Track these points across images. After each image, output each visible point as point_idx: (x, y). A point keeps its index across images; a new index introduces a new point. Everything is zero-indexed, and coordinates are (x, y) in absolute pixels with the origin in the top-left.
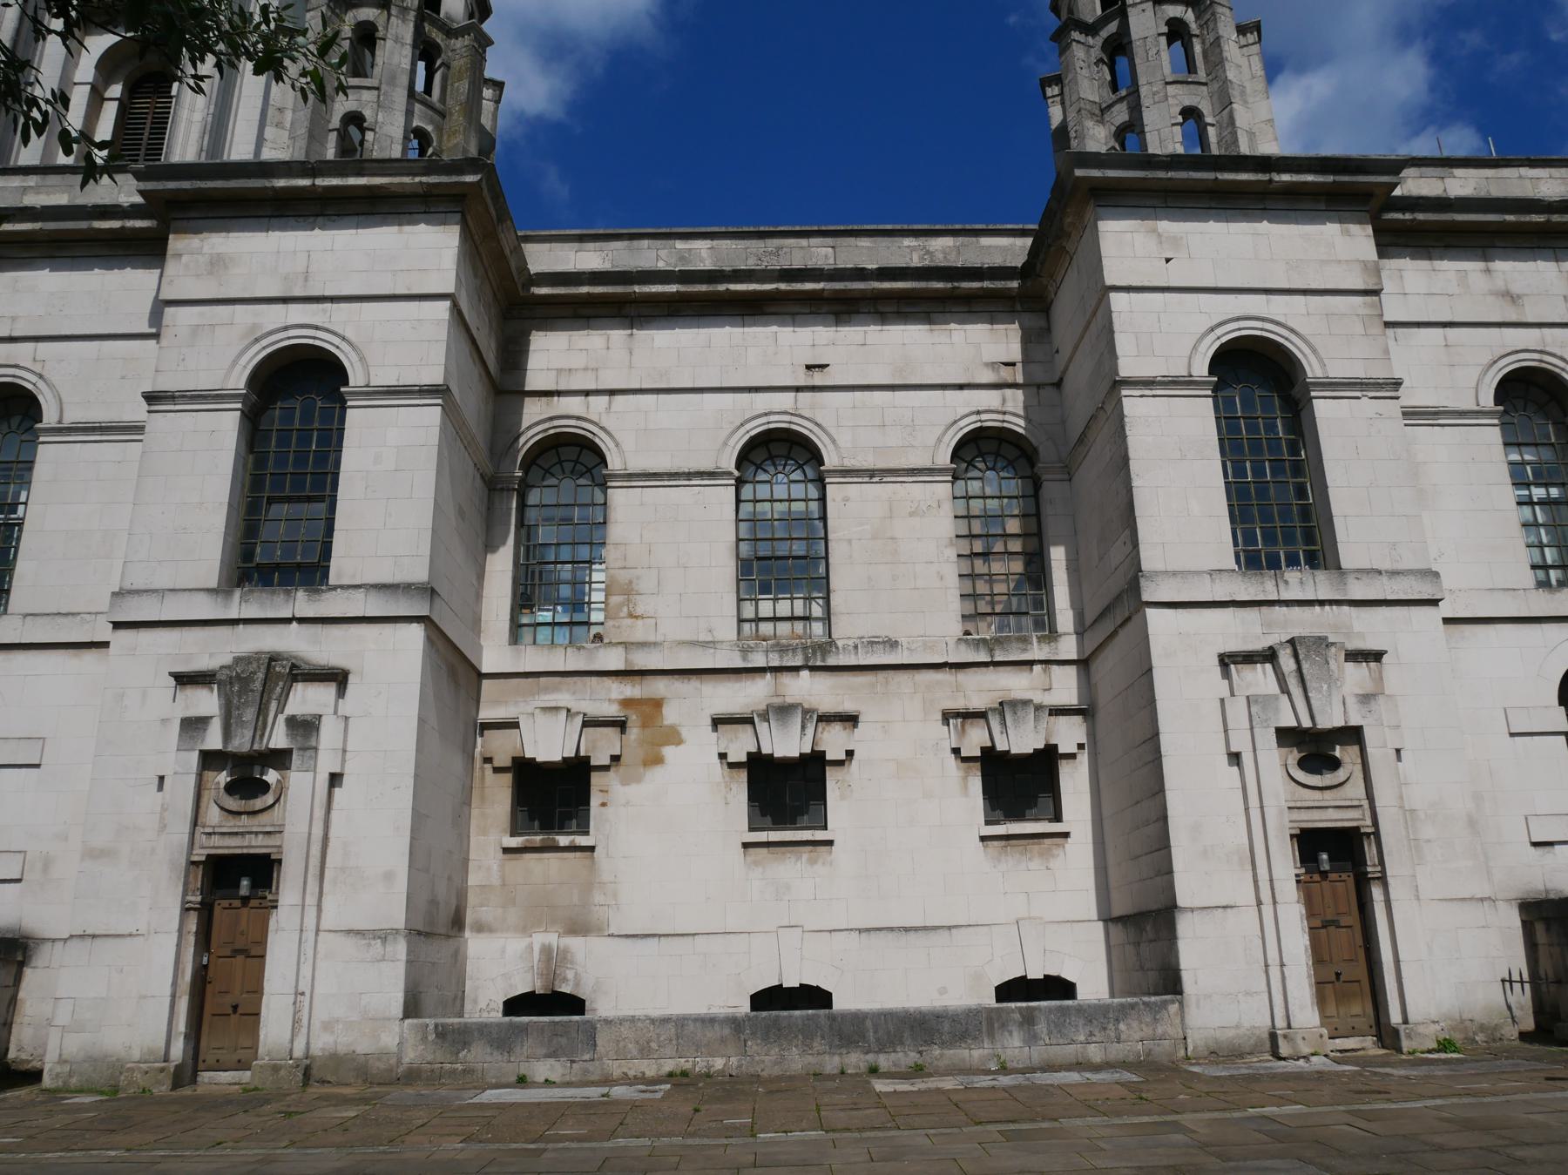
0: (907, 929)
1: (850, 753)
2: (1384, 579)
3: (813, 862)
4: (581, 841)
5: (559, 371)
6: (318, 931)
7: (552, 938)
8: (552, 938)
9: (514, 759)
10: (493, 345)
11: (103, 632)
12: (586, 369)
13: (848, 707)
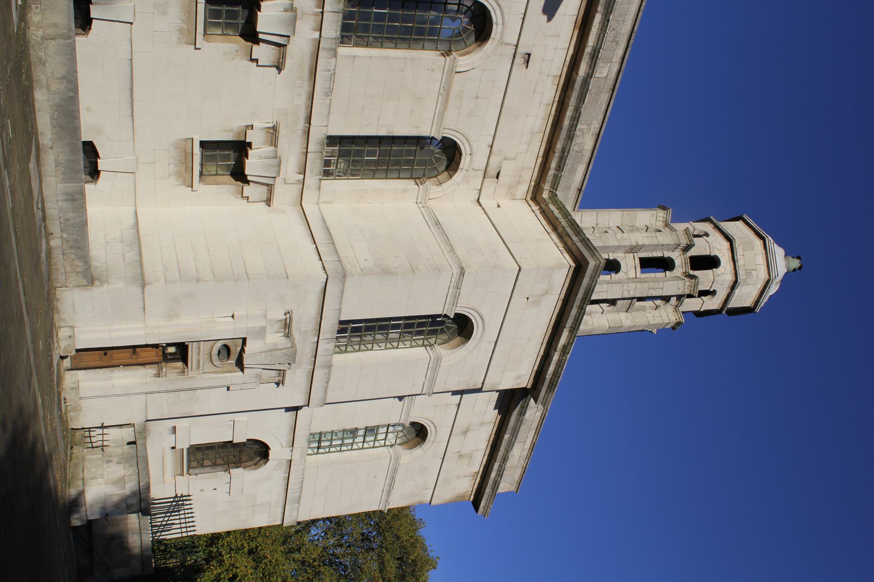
0: (132, 89)
2: (324, 384)
3: (181, 31)
9: (250, 145)
13: (289, 62)
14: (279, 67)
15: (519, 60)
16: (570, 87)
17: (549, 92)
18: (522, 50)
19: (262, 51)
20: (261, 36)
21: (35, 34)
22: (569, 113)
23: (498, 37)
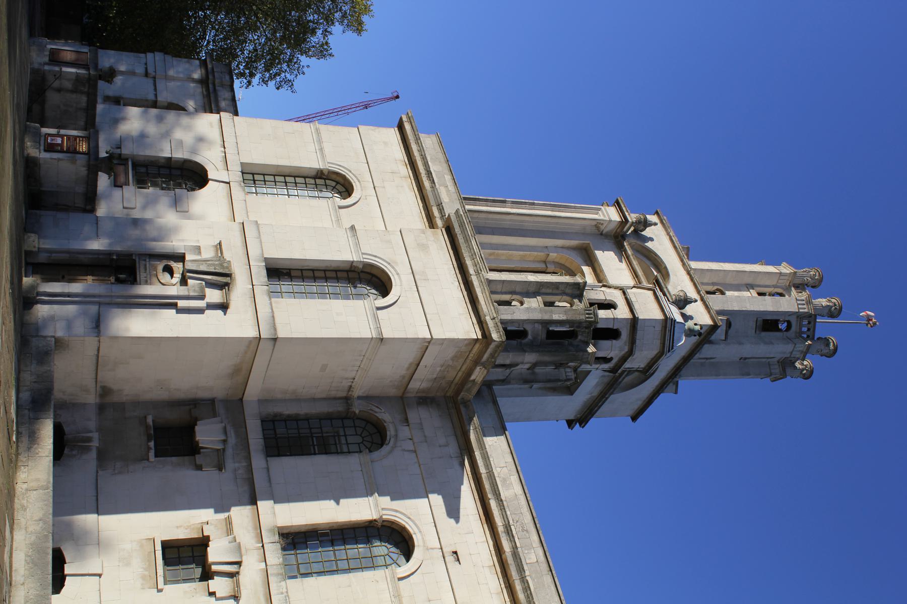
1: (212, 594)
3: (143, 577)
4: (152, 454)
5: (421, 424)
6: (100, 304)
7: (95, 444)
8: (95, 444)
10: (425, 385)
11: (239, 219)
12: (425, 436)
14: (236, 598)
15: (450, 559)
16: (507, 566)
17: (493, 582)
18: (448, 550)
19: (219, 584)
20: (214, 568)
21: (20, 487)
22: (518, 587)
23: (421, 543)
